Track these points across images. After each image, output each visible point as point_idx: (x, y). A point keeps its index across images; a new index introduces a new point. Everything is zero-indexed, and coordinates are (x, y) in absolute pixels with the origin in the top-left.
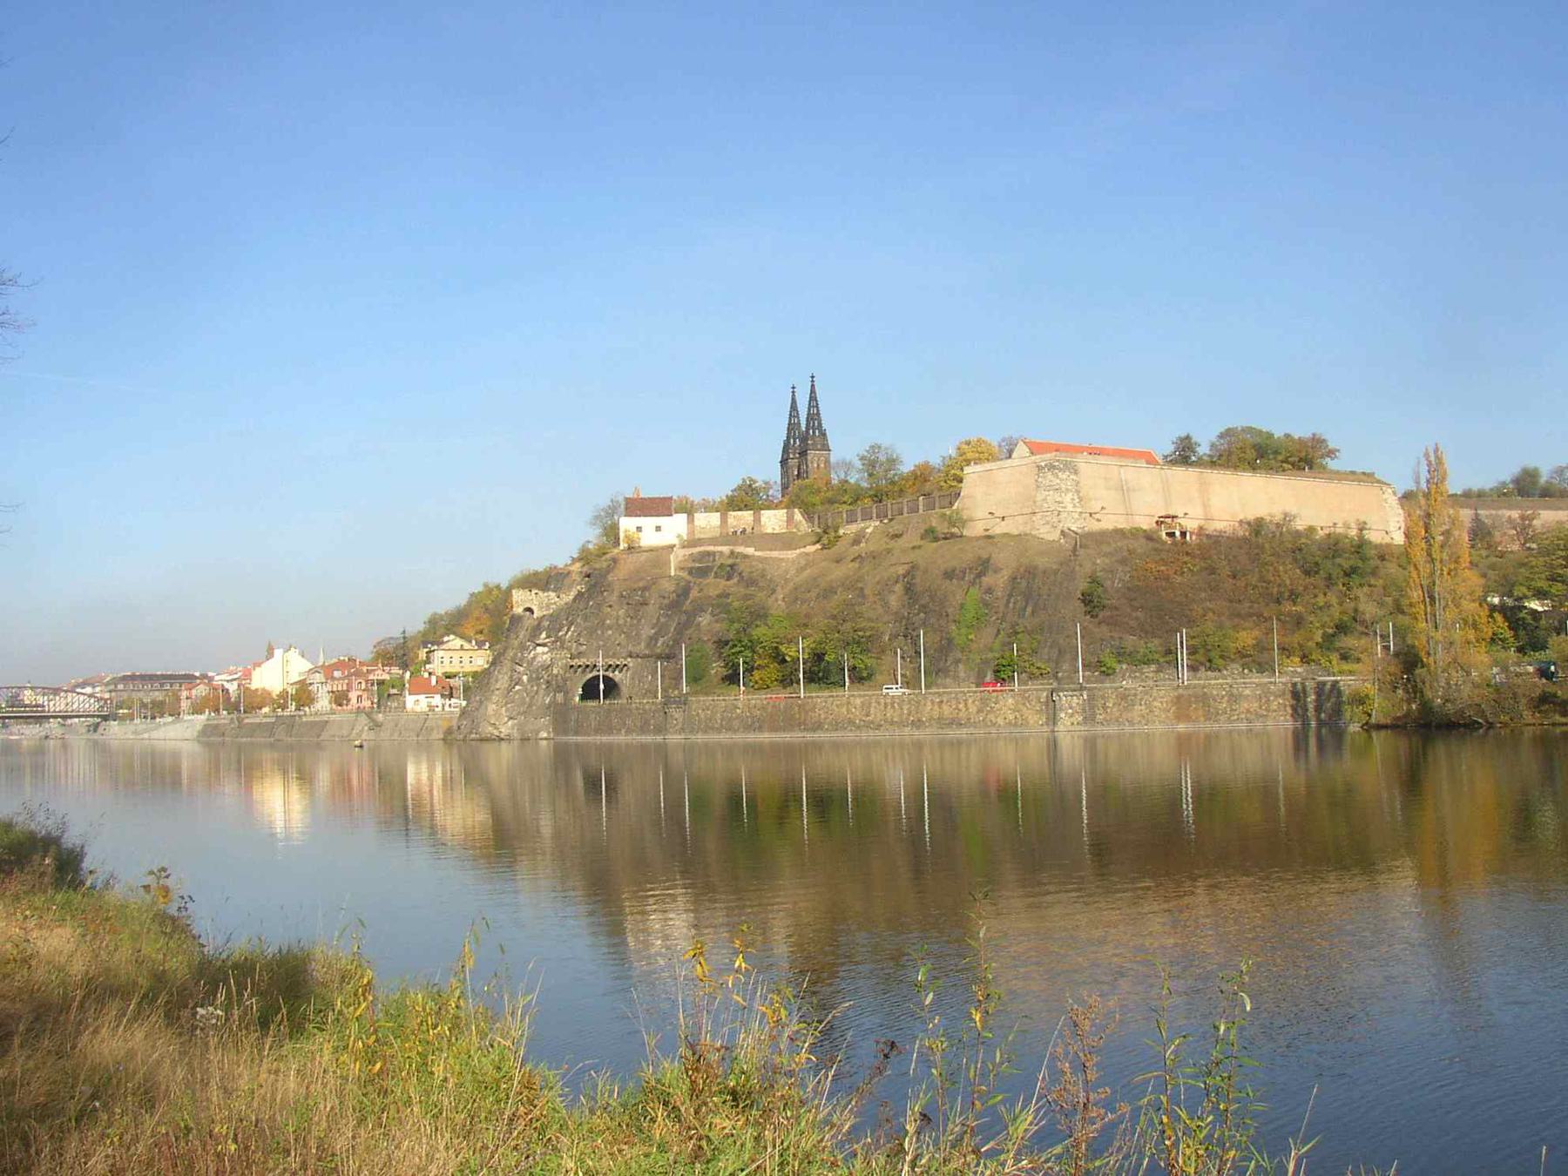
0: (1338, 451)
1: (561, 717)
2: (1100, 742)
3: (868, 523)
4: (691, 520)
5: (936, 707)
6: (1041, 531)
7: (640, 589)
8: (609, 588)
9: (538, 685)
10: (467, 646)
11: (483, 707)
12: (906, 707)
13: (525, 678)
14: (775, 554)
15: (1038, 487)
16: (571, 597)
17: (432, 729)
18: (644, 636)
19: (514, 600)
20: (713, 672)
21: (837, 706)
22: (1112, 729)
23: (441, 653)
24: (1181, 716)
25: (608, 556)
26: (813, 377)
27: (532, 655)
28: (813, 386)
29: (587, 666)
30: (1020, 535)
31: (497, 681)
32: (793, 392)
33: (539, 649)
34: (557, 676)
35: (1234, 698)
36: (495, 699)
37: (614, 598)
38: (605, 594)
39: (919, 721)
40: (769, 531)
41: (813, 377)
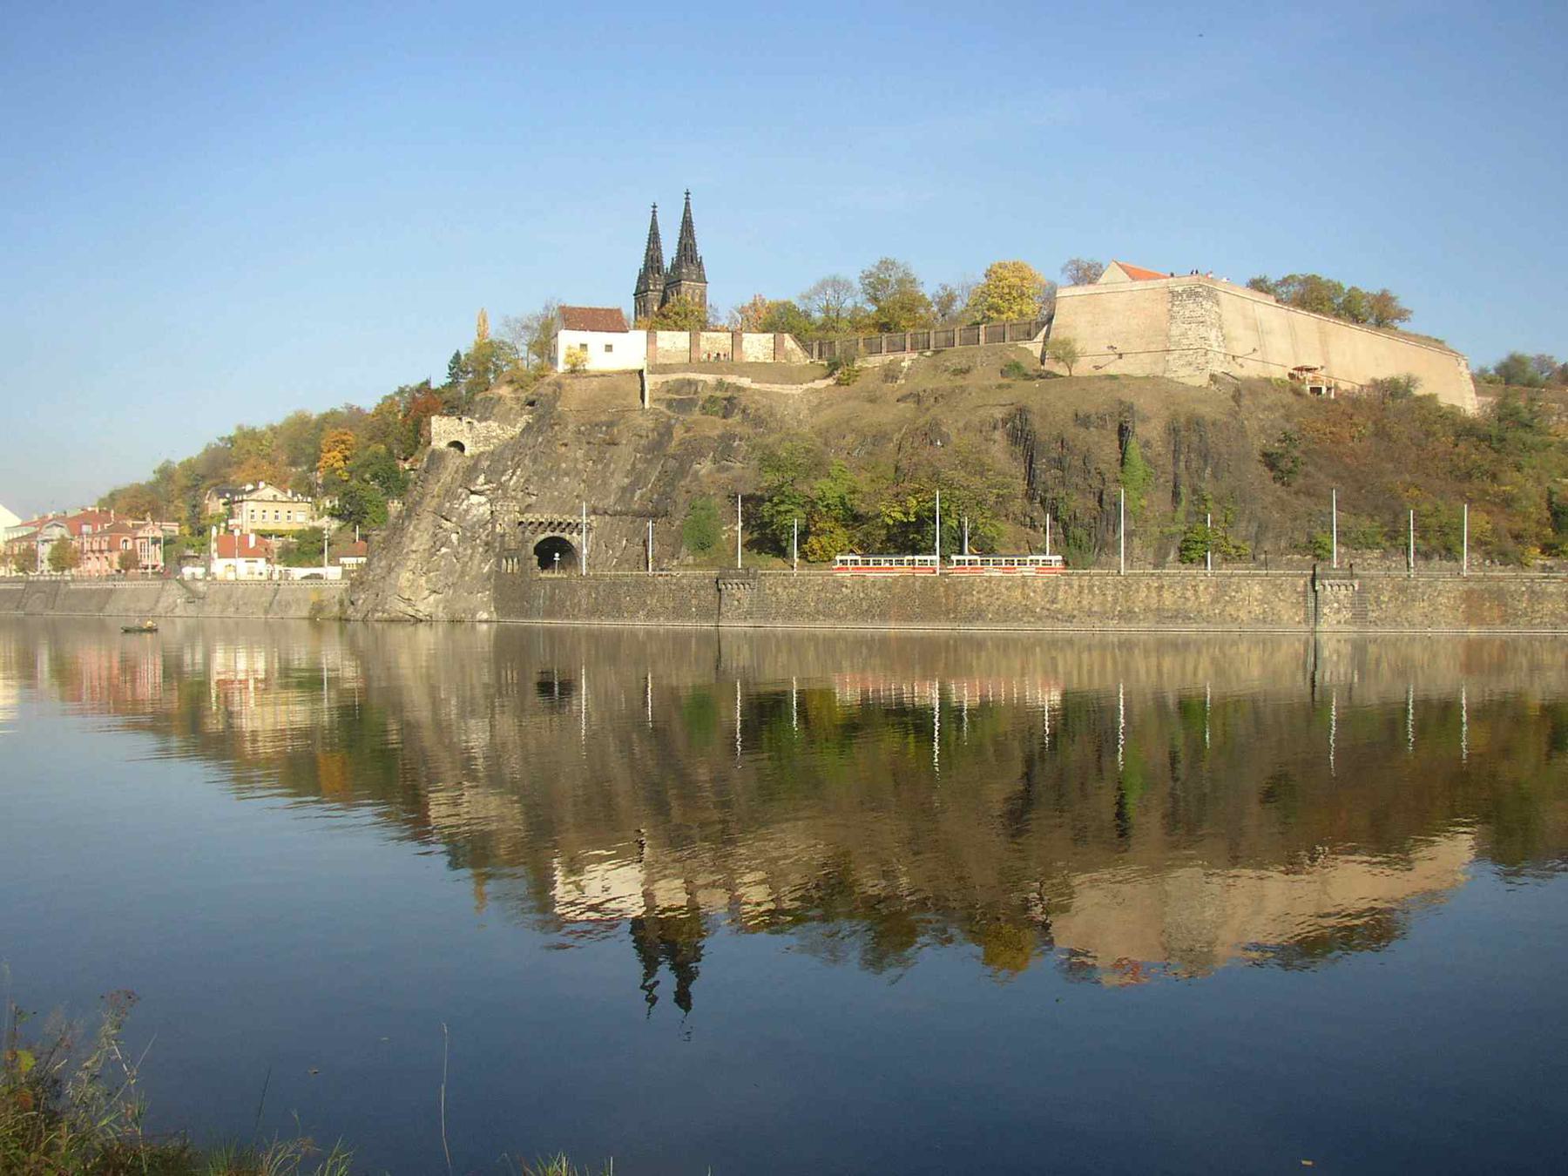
0: (1411, 312)
1: (510, 595)
2: (1372, 649)
3: (899, 355)
4: (651, 340)
5: (1154, 594)
6: (1180, 373)
7: (603, 424)
8: (560, 420)
9: (473, 548)
10: (280, 496)
11: (393, 575)
12: (1110, 593)
13: (454, 537)
14: (776, 388)
15: (1172, 317)
16: (518, 430)
17: (288, 604)
18: (614, 486)
19: (433, 431)
20: (723, 537)
21: (1008, 589)
22: (1388, 631)
23: (251, 505)
24: (1470, 618)
25: (547, 380)
26: (688, 194)
27: (464, 506)
28: (687, 204)
29: (541, 523)
30: (1147, 377)
31: (413, 540)
32: (654, 212)
33: (474, 499)
34: (503, 536)
35: (1535, 596)
36: (411, 564)
37: (569, 435)
38: (556, 428)
39: (1129, 612)
40: (751, 359)
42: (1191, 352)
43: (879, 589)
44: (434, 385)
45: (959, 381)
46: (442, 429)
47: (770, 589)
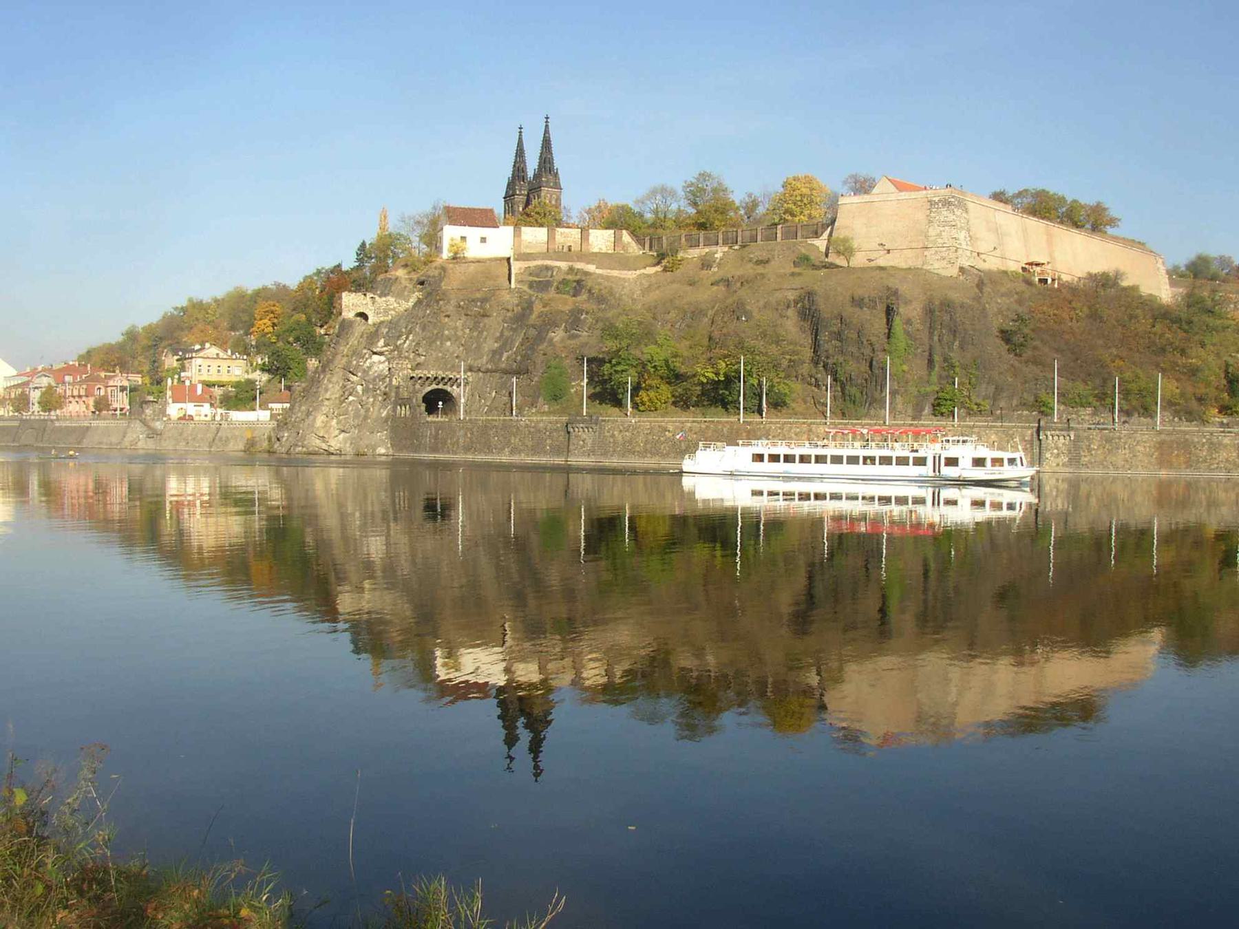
0: (1119, 220)
1: (402, 433)
2: (1084, 488)
3: (714, 248)
4: (517, 234)
6: (936, 265)
7: (478, 300)
8: (444, 296)
9: (374, 397)
10: (222, 355)
11: (311, 418)
13: (359, 388)
14: (615, 273)
15: (930, 222)
16: (411, 304)
17: (227, 439)
18: (486, 349)
19: (343, 304)
20: (572, 391)
22: (1098, 472)
23: (199, 361)
24: (1163, 462)
25: (434, 265)
27: (367, 364)
28: (547, 126)
29: (428, 378)
30: (910, 269)
31: (326, 390)
32: (520, 132)
33: (376, 358)
34: (398, 388)
35: (1214, 447)
36: (324, 409)
37: (450, 308)
38: (441, 303)
40: (596, 250)
41: (547, 118)
42: (945, 249)
43: (696, 433)
44: (345, 268)
45: (760, 269)
46: (351, 303)
47: (608, 432)
